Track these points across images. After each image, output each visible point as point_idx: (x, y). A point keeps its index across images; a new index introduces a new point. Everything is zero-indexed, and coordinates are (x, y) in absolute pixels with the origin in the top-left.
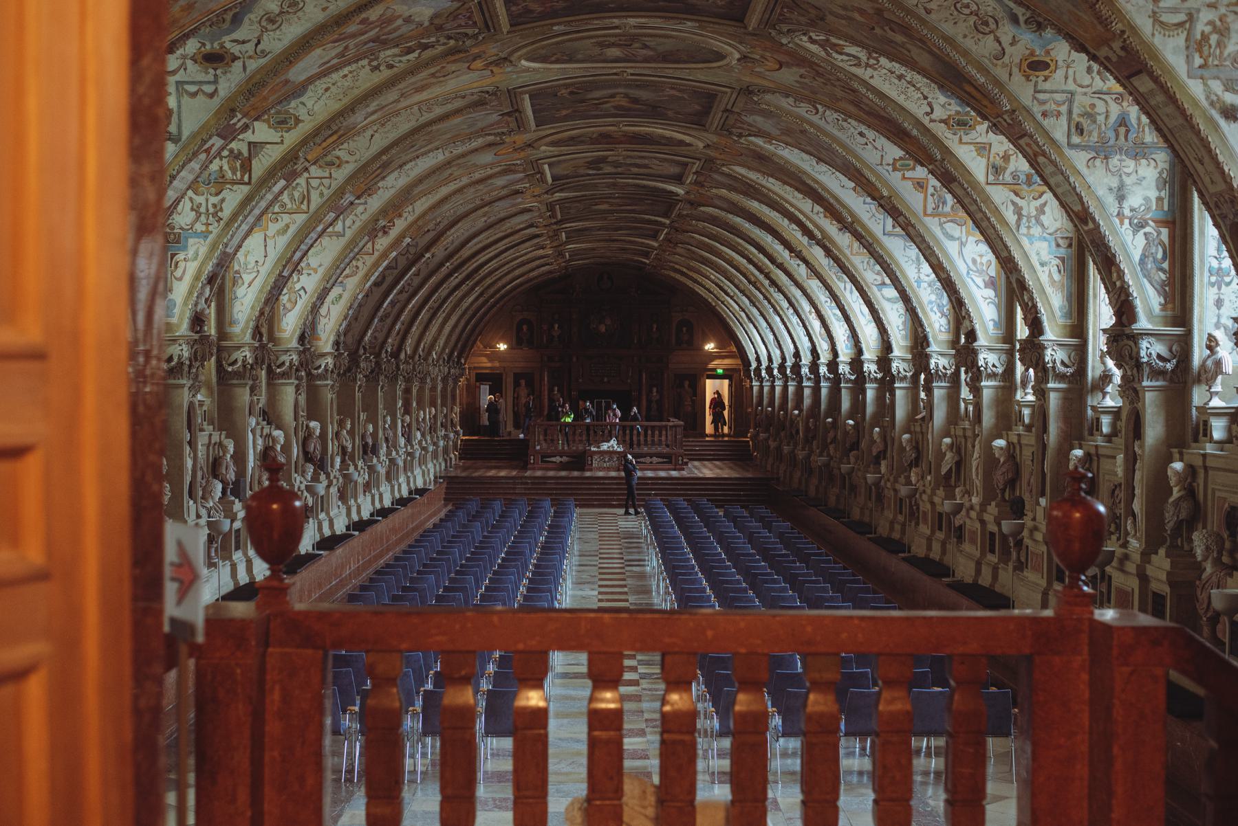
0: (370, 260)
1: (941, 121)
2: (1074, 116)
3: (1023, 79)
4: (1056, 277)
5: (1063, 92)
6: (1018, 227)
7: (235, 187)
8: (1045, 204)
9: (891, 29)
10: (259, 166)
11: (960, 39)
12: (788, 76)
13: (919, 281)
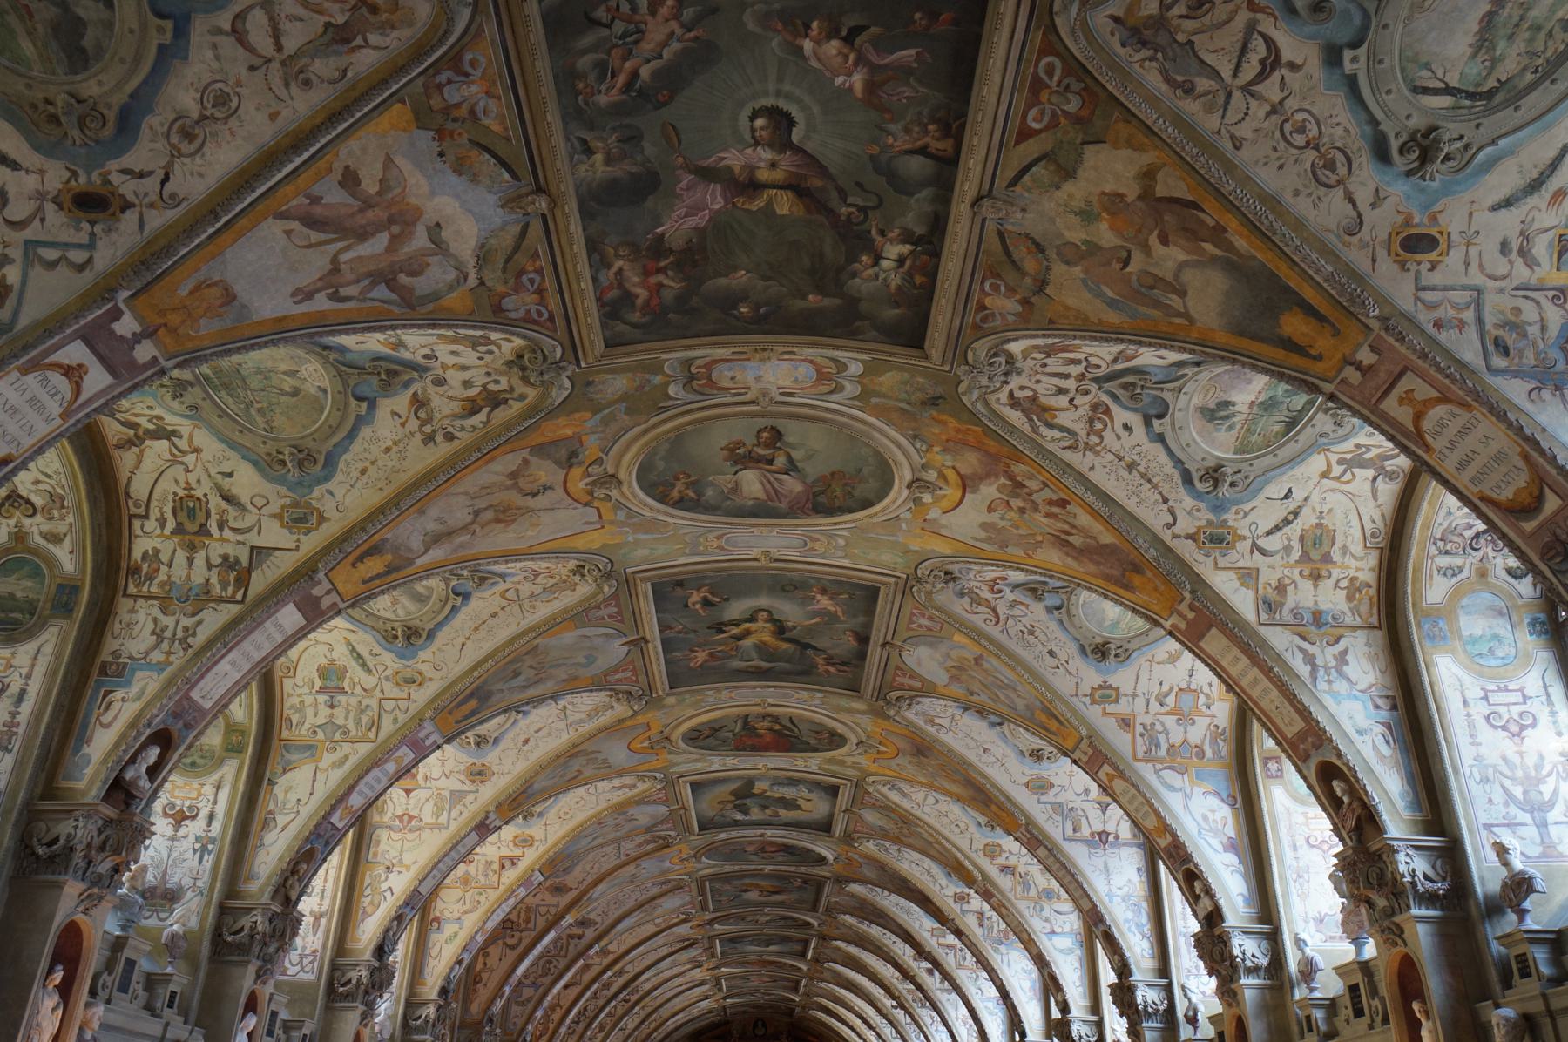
0: (493, 895)
1: (1188, 537)
2: (1488, 327)
3: (1396, 266)
4: (1385, 750)
5: (1464, 288)
6: (1315, 680)
7: (222, 606)
8: (1345, 652)
9: (1164, 241)
10: (260, 582)
11: (1288, 198)
12: (968, 518)
13: (1110, 895)
